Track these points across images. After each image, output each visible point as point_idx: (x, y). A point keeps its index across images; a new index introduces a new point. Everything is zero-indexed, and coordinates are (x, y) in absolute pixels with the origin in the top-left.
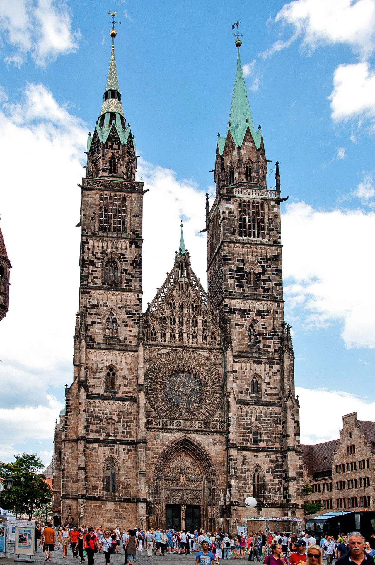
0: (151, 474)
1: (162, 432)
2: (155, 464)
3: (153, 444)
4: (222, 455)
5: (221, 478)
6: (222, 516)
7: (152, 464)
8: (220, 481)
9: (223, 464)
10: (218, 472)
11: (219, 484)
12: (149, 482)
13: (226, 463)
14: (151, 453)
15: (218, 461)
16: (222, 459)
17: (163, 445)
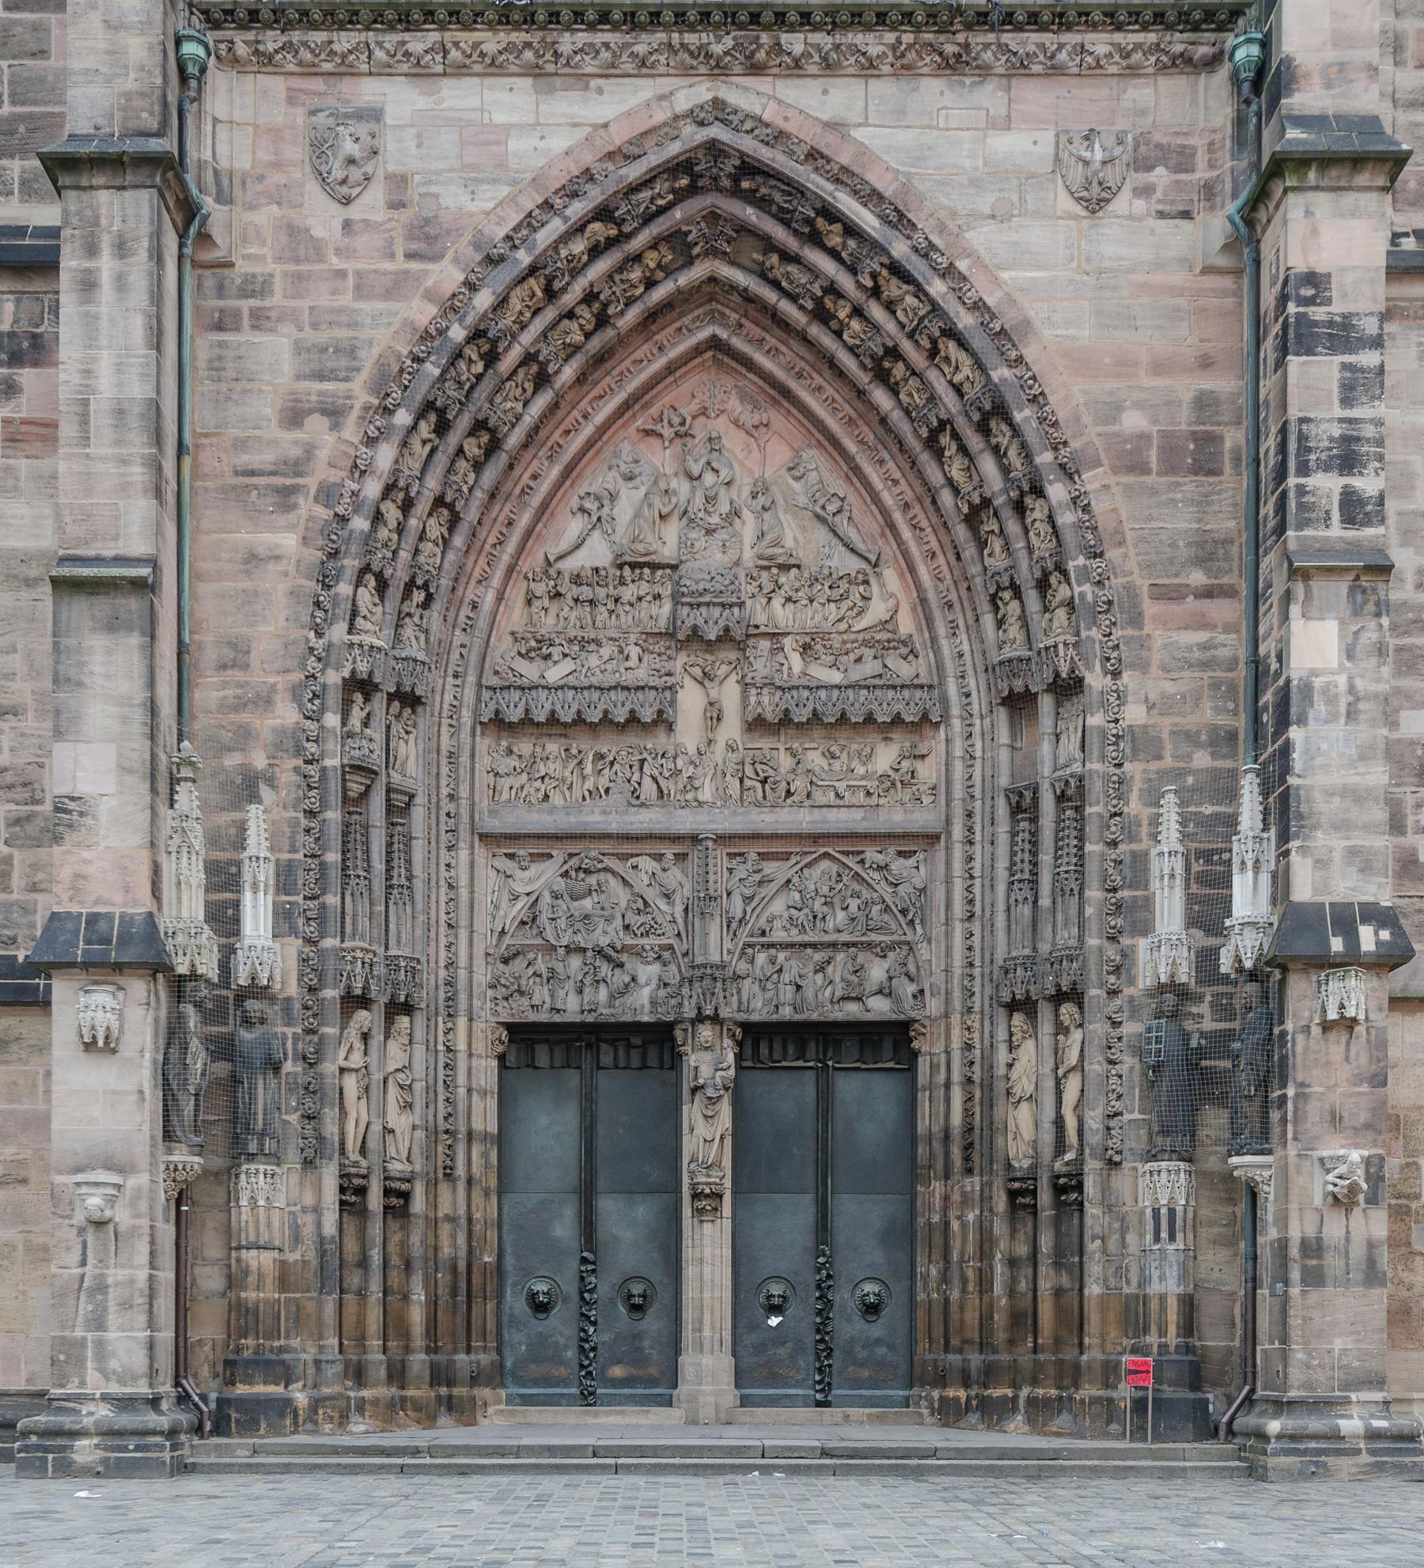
0: (273, 626)
1: (419, 72)
2: (327, 494)
3: (297, 241)
4: (1186, 339)
5: (1169, 635)
6: (1175, 1135)
7: (286, 497)
8: (1158, 683)
9: (1199, 456)
10: (1128, 565)
11: (1134, 714)
12: (244, 736)
13: (1234, 438)
14: (273, 356)
15: (1133, 421)
16: (1186, 387)
17: (426, 241)
